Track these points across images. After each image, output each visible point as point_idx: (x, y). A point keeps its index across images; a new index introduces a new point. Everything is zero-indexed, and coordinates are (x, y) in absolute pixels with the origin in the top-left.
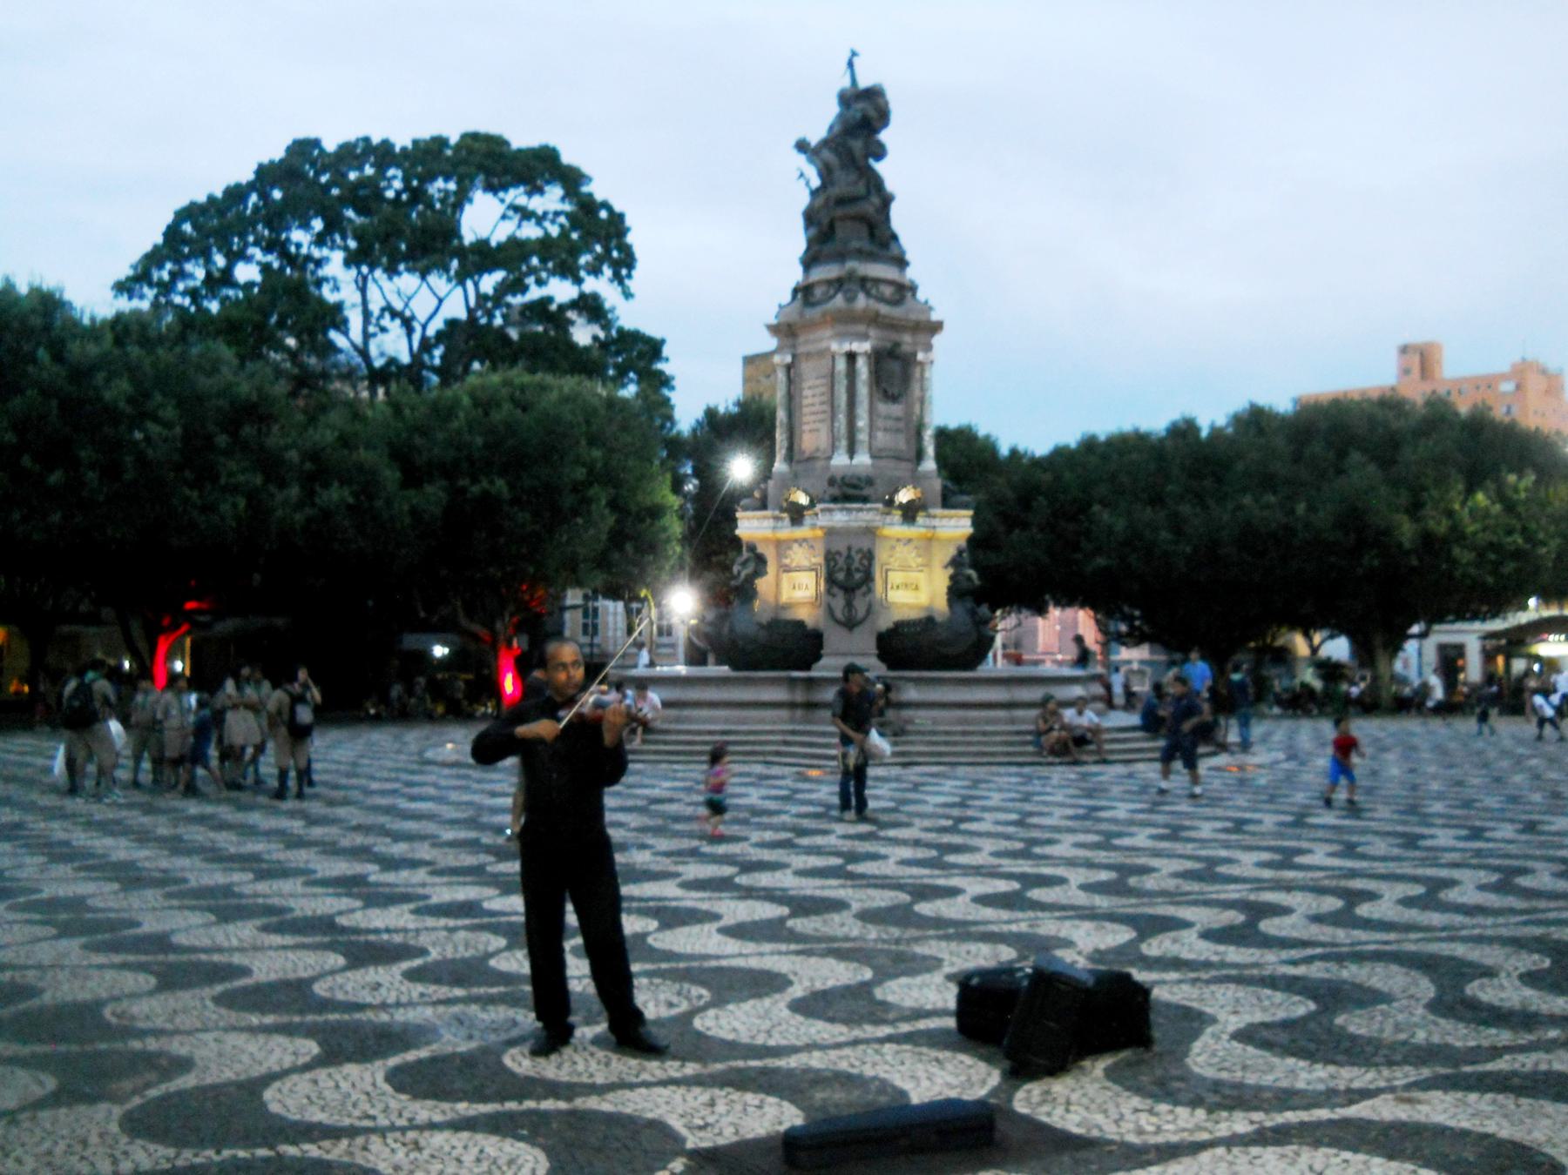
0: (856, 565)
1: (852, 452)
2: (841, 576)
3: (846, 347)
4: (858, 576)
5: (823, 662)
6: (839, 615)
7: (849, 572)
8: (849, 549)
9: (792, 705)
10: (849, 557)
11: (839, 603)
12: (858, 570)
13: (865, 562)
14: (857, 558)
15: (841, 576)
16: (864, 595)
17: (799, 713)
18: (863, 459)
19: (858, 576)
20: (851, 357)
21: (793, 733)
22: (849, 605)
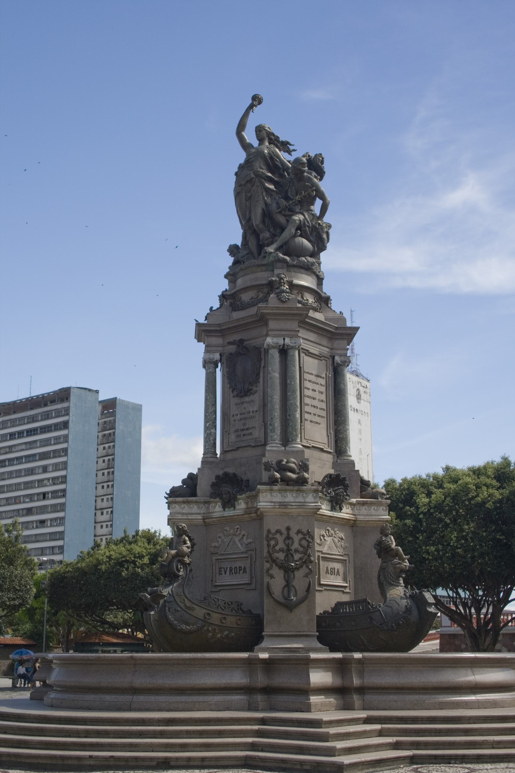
0: (296, 545)
2: (281, 556)
3: (281, 342)
4: (297, 556)
5: (263, 645)
8: (288, 529)
9: (247, 690)
10: (288, 537)
11: (277, 582)
12: (296, 551)
13: (304, 543)
14: (296, 538)
15: (281, 556)
17: (259, 698)
19: (297, 556)
21: (263, 721)
22: (288, 585)
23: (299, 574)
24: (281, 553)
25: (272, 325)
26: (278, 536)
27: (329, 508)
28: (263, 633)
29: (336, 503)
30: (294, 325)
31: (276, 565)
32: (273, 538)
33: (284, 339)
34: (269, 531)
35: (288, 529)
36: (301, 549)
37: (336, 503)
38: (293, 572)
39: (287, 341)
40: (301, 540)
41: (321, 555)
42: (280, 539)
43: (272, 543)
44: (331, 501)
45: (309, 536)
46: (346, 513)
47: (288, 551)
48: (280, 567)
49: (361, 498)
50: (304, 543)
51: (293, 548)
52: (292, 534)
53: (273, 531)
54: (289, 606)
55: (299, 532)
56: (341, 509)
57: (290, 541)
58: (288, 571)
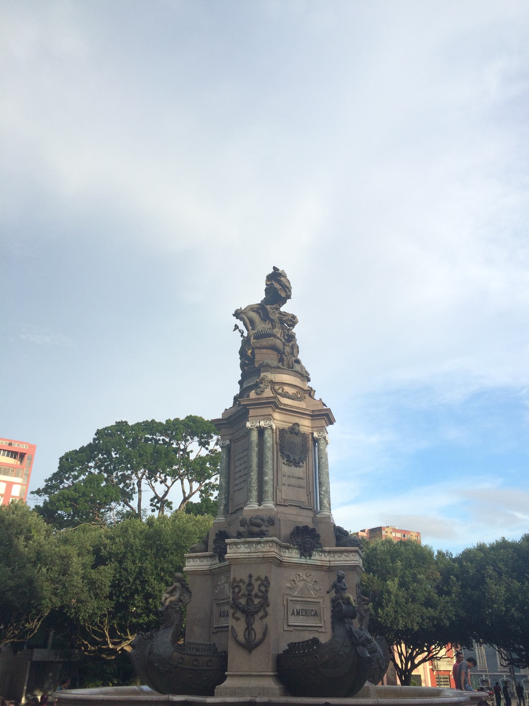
0: (255, 591)
1: (260, 501)
2: (243, 601)
4: (256, 601)
6: (241, 638)
7: (250, 600)
8: (250, 576)
10: (250, 584)
12: (256, 596)
13: (263, 588)
14: (256, 584)
15: (243, 601)
16: (262, 618)
18: (270, 504)
19: (256, 601)
20: (261, 431)
23: (257, 617)
24: (244, 598)
25: (252, 412)
26: (241, 584)
27: (298, 556)
28: (226, 673)
29: (306, 552)
30: (269, 411)
31: (240, 610)
32: (238, 586)
33: (259, 422)
34: (234, 579)
35: (250, 576)
36: (260, 594)
37: (306, 552)
38: (252, 615)
39: (262, 424)
40: (260, 586)
41: (290, 598)
42: (243, 587)
43: (237, 590)
44: (299, 549)
45: (266, 583)
46: (317, 558)
47: (249, 598)
48: (243, 611)
49: (337, 546)
50: (263, 588)
51: (253, 593)
52: (253, 582)
53: (238, 580)
54: (249, 646)
55: (258, 579)
56: (310, 556)
57: (251, 587)
58: (249, 614)
